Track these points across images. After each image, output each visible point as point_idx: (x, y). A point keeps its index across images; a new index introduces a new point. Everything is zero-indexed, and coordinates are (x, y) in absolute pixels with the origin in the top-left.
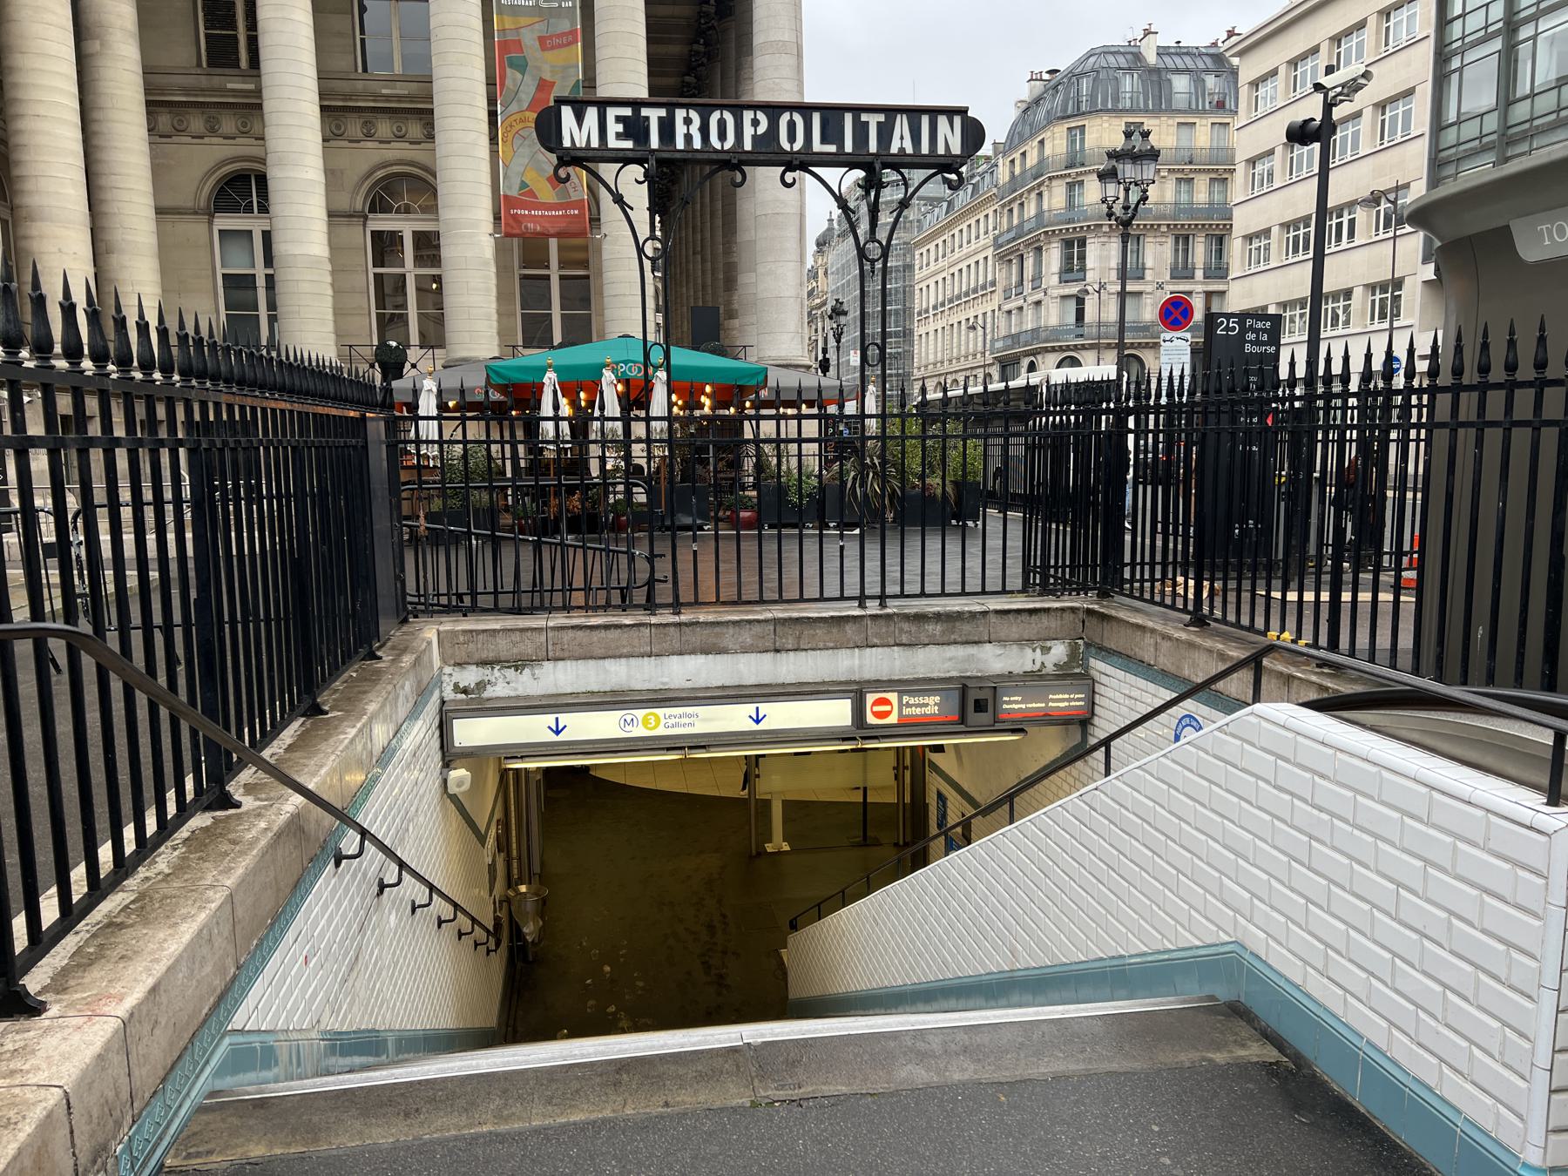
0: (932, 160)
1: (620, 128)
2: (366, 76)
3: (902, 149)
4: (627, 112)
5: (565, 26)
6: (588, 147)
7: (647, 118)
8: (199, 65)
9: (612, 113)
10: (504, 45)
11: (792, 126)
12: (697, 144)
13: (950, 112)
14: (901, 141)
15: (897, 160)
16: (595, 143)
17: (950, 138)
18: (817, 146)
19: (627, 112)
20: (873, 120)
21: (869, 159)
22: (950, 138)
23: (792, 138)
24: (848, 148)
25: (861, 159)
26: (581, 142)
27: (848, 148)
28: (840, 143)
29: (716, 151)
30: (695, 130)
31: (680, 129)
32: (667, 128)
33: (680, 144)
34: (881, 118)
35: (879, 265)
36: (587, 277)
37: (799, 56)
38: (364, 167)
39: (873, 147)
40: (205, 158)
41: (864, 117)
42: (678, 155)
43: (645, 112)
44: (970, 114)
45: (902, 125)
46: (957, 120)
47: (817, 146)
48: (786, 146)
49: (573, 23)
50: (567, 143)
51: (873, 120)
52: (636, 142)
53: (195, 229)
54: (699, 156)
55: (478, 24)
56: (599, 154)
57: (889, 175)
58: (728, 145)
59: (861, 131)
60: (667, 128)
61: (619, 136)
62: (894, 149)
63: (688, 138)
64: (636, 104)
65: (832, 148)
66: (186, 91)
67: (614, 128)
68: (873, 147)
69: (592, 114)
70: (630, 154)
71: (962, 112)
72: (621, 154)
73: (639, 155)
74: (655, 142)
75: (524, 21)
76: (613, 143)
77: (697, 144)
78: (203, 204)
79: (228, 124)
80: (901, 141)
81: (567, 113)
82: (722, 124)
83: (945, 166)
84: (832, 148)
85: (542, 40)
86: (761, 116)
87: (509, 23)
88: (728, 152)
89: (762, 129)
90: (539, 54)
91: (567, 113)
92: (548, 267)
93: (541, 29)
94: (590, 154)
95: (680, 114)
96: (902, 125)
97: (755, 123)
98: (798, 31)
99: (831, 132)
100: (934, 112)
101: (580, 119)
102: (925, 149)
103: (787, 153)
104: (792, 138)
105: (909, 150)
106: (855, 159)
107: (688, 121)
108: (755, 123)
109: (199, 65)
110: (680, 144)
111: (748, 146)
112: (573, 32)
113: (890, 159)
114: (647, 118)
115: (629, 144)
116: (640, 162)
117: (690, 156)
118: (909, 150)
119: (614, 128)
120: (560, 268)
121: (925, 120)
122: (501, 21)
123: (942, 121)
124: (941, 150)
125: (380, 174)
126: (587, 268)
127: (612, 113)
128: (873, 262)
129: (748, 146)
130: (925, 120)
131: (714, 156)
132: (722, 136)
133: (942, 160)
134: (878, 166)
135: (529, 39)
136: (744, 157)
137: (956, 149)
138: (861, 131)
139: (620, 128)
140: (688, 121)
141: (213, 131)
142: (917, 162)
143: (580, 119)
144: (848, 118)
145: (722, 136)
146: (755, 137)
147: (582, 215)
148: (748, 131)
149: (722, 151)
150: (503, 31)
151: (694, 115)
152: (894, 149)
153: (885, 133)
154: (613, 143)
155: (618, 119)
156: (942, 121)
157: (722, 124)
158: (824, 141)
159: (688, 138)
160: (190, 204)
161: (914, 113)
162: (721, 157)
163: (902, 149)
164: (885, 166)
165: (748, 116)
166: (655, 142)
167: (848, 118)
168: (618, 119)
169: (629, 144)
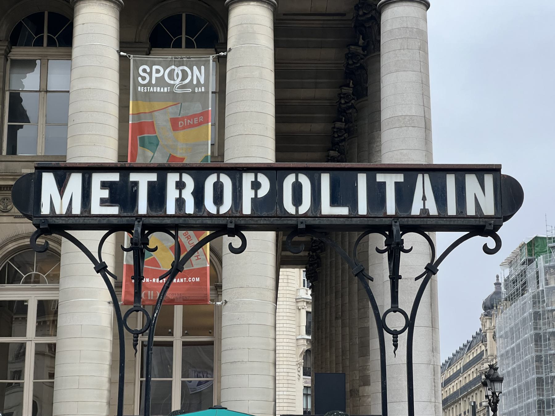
0: (460, 222)
1: (106, 194)
2: (10, 158)
3: (425, 211)
4: (115, 177)
5: (197, 108)
6: (69, 214)
7: (136, 184)
9: (97, 179)
10: (140, 128)
11: (297, 189)
12: (190, 208)
13: (480, 171)
14: (424, 200)
15: (418, 222)
16: (77, 210)
17: (481, 198)
18: (326, 208)
19: (115, 177)
21: (387, 221)
22: (481, 198)
23: (297, 200)
24: (363, 209)
25: (377, 222)
26: (61, 209)
27: (363, 209)
28: (354, 205)
29: (211, 216)
30: (188, 195)
31: (172, 194)
32: (157, 194)
33: (171, 209)
34: (400, 178)
35: (403, 338)
36: (211, 343)
37: (427, 128)
39: (391, 208)
41: (380, 178)
42: (168, 221)
43: (134, 177)
44: (503, 172)
45: (423, 186)
46: (489, 179)
47: (326, 208)
48: (290, 208)
49: (205, 105)
50: (45, 210)
51: (390, 181)
52: (123, 208)
54: (191, 221)
55: (113, 109)
56: (81, 221)
57: (411, 239)
58: (225, 208)
59: (377, 194)
60: (157, 194)
61: (103, 202)
62: (416, 210)
63: (180, 202)
65: (344, 211)
67: (98, 193)
68: (391, 208)
70: (115, 221)
71: (495, 170)
72: (105, 221)
73: (124, 221)
74: (143, 207)
75: (157, 105)
76: (96, 209)
77: (190, 208)
80: (424, 200)
81: (48, 181)
82: (218, 189)
83: (483, 227)
84: (344, 211)
85: (175, 124)
86: (263, 180)
87: (144, 107)
88: (224, 216)
89: (263, 192)
90: (170, 134)
91: (48, 181)
92: (171, 334)
93: (173, 112)
94: (71, 221)
95: (172, 178)
96: (423, 186)
97: (256, 186)
98: (426, 106)
100: (460, 171)
101: (62, 185)
102: (452, 210)
103: (291, 216)
104: (297, 200)
105: (433, 210)
106: (371, 222)
107: (180, 186)
108: (256, 186)
110: (171, 209)
111: (247, 209)
112: (205, 114)
113: (411, 222)
114: (136, 184)
115: (114, 210)
116: (128, 228)
117: (181, 221)
118: (433, 210)
119: (98, 193)
120: (184, 334)
121: (451, 181)
122: (136, 106)
123: (471, 181)
124: (471, 211)
125: (11, 246)
126: (211, 334)
127: (97, 179)
128: (395, 334)
129: (247, 209)
130: (451, 181)
131: (208, 221)
132: (218, 200)
133: (473, 222)
134: (395, 229)
135: (162, 122)
136: (242, 222)
137: (489, 209)
138: (377, 194)
139: (106, 194)
140: (180, 186)
142: (445, 224)
143: (62, 185)
144: (362, 180)
145: (218, 200)
146: (255, 201)
147: (203, 282)
148: (248, 194)
149: (218, 216)
150: (137, 114)
151: (188, 180)
152: (416, 210)
153: (405, 194)
154: (96, 209)
155: (104, 185)
156: (471, 181)
157: (218, 189)
158: (334, 202)
159: (180, 202)
161: (438, 173)
162: (216, 221)
163: (425, 211)
164: (407, 229)
165: (248, 179)
166: (143, 207)
167: (362, 180)
168: (104, 185)
169: (114, 210)
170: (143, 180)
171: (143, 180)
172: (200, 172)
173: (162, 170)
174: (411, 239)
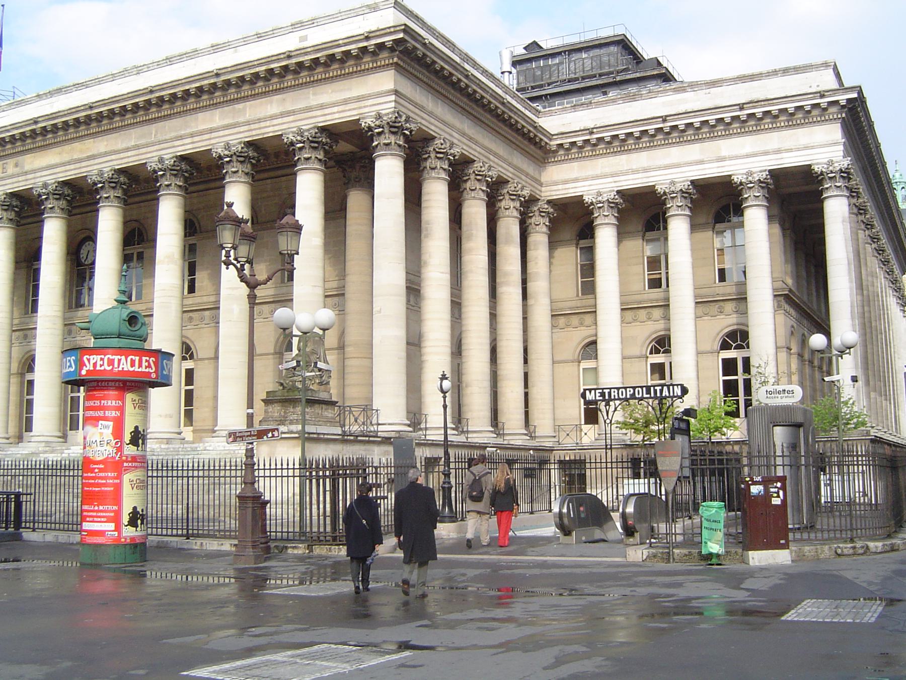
8: (578, 295)
13: (677, 385)
17: (678, 391)
20: (658, 388)
32: (610, 393)
38: (647, 333)
39: (658, 395)
40: (577, 336)
45: (665, 388)
47: (645, 396)
51: (658, 388)
53: (570, 368)
59: (655, 391)
60: (610, 393)
64: (603, 389)
66: (571, 309)
67: (598, 395)
68: (658, 395)
69: (593, 392)
71: (682, 385)
78: (576, 357)
79: (588, 319)
80: (665, 393)
81: (587, 392)
91: (587, 392)
96: (665, 388)
99: (648, 392)
109: (578, 295)
119: (598, 395)
137: (679, 394)
138: (655, 391)
141: (581, 324)
148: (628, 393)
154: (598, 398)
160: (571, 358)
170: (607, 391)
171: (607, 391)
172: (618, 389)
173: (610, 389)
174: (664, 401)
